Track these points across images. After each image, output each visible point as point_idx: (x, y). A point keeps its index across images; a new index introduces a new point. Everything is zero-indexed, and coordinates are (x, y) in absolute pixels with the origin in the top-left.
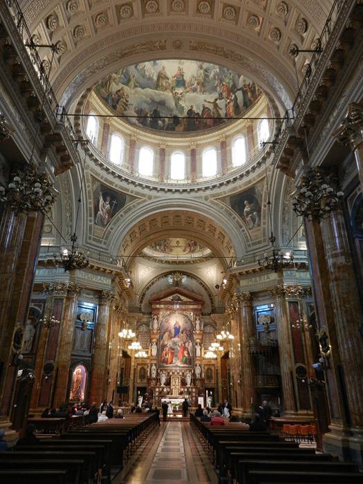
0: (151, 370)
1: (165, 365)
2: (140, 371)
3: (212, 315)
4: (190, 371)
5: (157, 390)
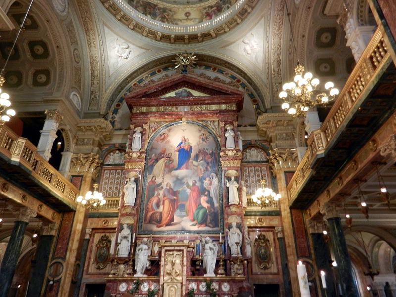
1: (155, 228)
5: (123, 287)
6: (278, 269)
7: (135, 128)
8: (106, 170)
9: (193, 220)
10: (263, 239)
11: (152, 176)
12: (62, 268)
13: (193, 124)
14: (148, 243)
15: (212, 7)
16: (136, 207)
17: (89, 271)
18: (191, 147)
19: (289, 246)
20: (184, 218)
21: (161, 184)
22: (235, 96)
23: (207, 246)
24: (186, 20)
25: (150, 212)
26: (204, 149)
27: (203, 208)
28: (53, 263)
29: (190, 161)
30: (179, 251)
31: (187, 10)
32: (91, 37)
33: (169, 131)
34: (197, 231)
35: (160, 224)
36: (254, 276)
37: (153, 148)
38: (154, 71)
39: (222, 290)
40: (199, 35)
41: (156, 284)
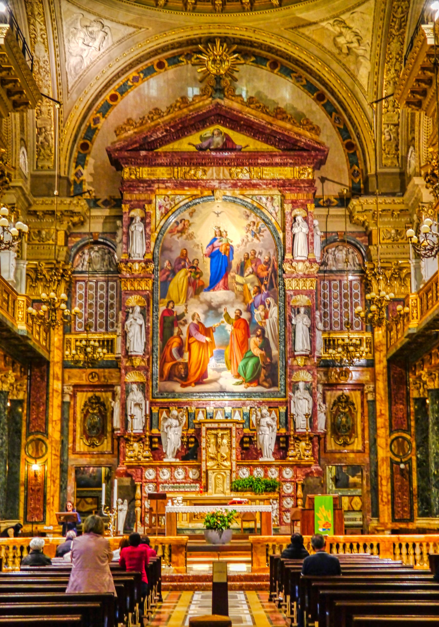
0: (124, 407)
1: (178, 388)
2: (86, 415)
3: (354, 202)
4: (272, 406)
6: (364, 444)
7: (130, 210)
8: (79, 281)
9: (239, 376)
10: (346, 402)
11: (167, 300)
12: (44, 447)
13: (234, 202)
14: (180, 417)
16: (147, 357)
17: (78, 449)
18: (232, 247)
19: (382, 415)
20: (224, 373)
21: (183, 315)
22: (313, 153)
23: (264, 421)
25: (169, 362)
26: (255, 254)
27: (253, 356)
28: (28, 440)
29: (232, 274)
30: (226, 429)
32: (38, 27)
33: (191, 214)
34: (244, 393)
35: (186, 381)
36: (329, 455)
37: (164, 249)
38: (150, 65)
39: (283, 477)
41: (194, 470)
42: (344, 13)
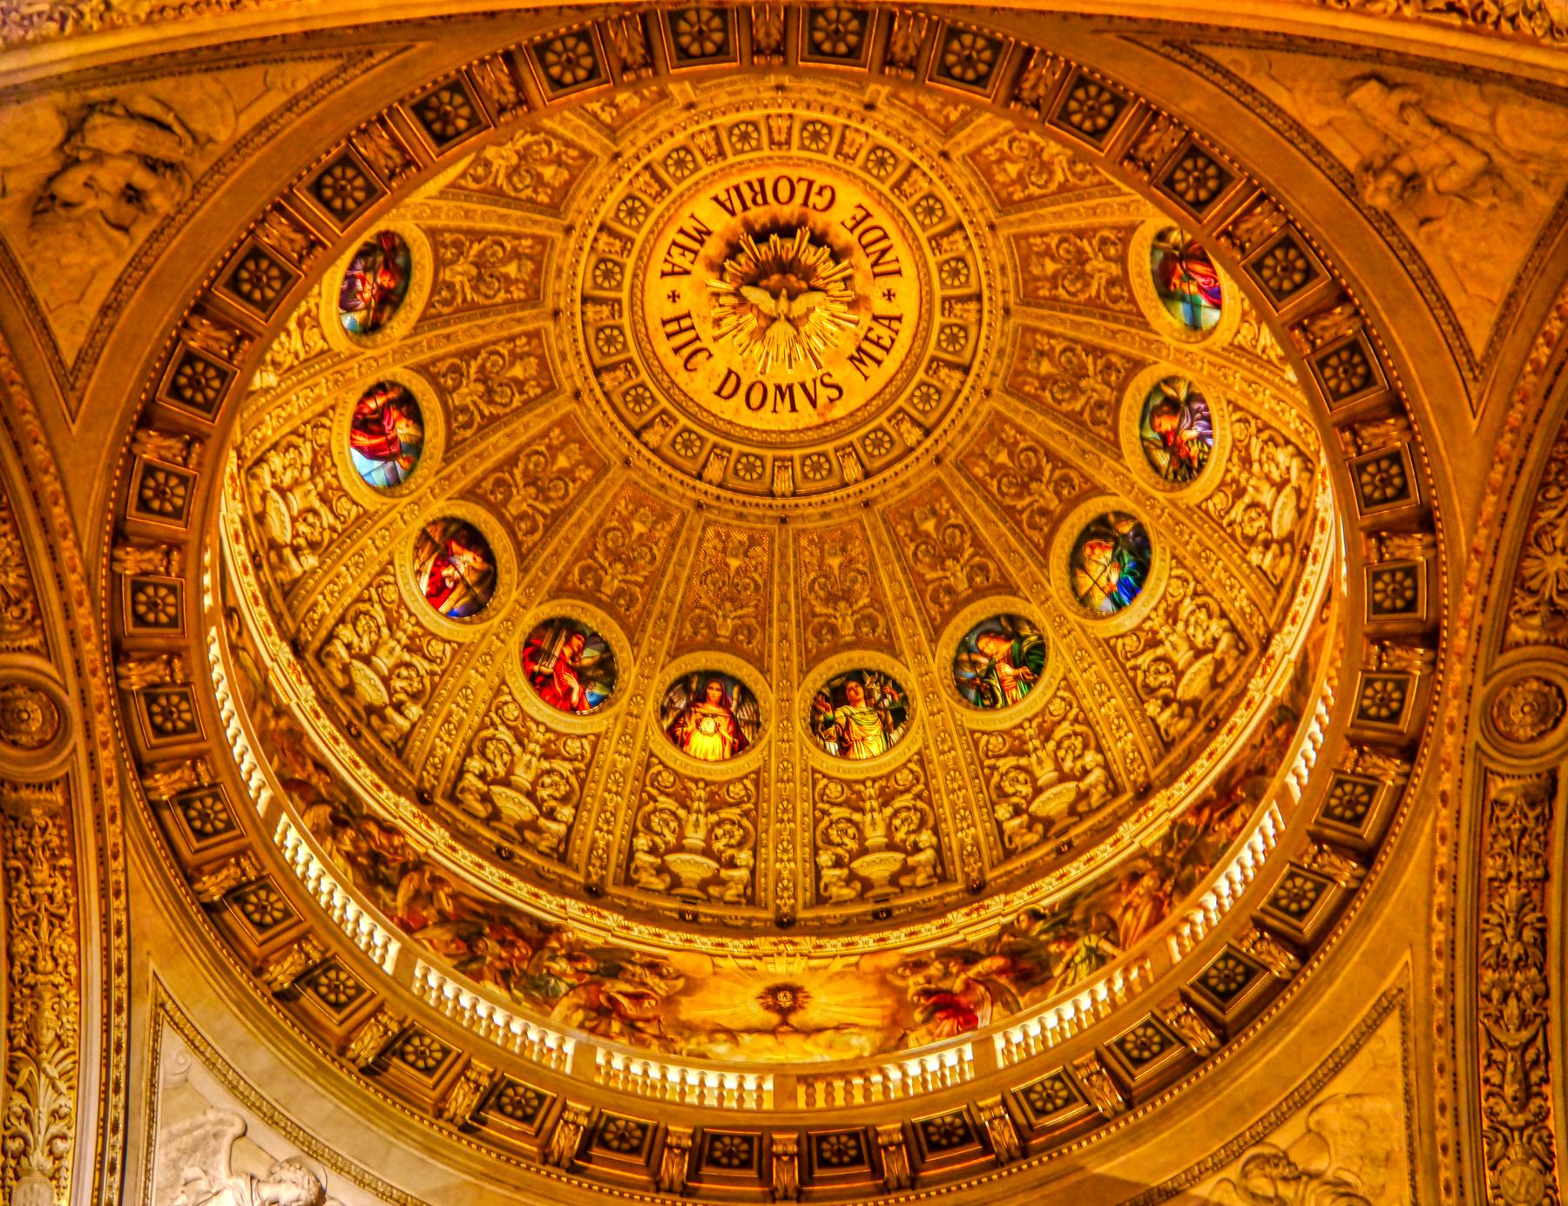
15: (968, 957)
24: (773, 1032)
31: (781, 969)
32: (46, 1100)
40: (890, 1128)
42: (1280, 1119)
